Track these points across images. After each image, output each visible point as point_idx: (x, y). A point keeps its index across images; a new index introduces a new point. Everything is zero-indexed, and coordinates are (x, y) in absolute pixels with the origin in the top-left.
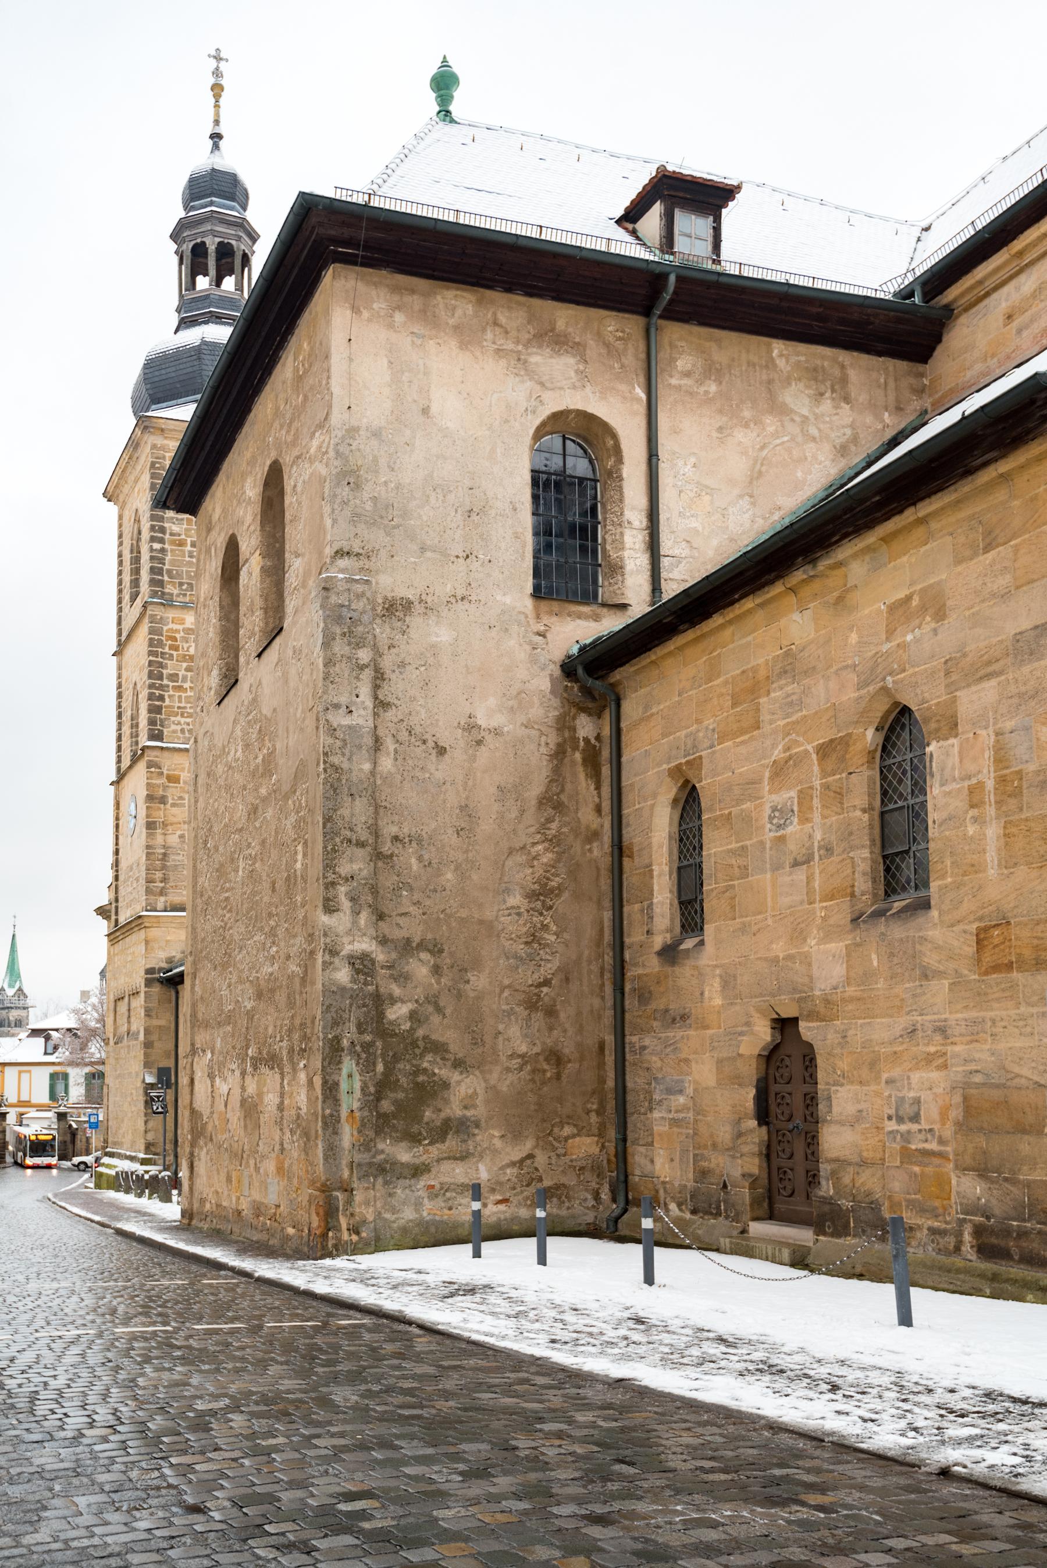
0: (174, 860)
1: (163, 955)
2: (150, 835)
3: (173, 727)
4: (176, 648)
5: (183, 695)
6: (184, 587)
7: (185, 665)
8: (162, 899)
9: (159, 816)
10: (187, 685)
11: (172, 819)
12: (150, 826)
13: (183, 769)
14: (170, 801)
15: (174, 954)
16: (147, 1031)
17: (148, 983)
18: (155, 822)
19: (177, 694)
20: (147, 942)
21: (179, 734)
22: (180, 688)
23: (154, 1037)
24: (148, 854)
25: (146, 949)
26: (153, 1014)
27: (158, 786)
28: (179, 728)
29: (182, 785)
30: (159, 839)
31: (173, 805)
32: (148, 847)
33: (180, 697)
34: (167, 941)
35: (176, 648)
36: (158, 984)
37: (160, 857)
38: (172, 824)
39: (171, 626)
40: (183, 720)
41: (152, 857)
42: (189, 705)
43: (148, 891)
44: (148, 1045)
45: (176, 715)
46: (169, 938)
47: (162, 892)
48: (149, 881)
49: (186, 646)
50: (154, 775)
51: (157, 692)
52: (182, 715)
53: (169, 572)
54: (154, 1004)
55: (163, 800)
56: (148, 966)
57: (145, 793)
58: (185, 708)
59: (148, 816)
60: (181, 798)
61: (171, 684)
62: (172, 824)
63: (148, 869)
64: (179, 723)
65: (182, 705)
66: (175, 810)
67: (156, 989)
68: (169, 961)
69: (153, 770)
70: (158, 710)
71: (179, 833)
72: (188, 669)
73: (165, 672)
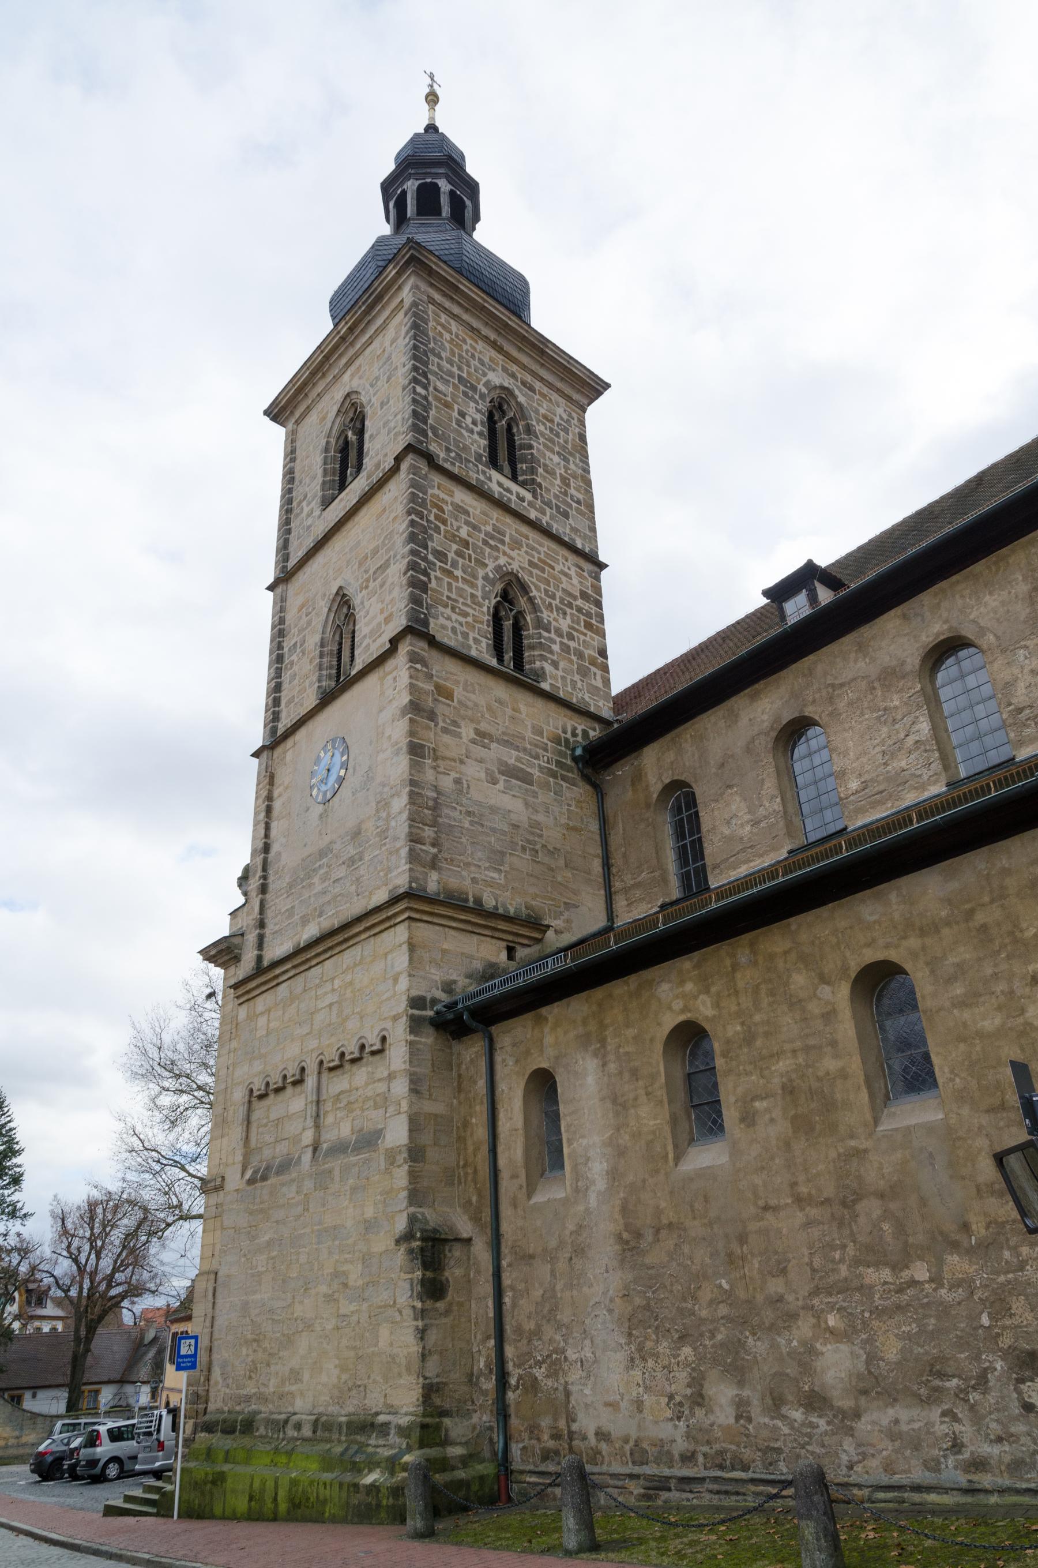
0: (449, 817)
1: (437, 975)
2: (415, 766)
3: (442, 621)
4: (444, 522)
5: (454, 584)
6: (453, 455)
7: (455, 547)
8: (434, 876)
9: (430, 737)
10: (458, 573)
11: (442, 751)
12: (416, 750)
13: (457, 682)
14: (441, 724)
15: (454, 977)
16: (415, 1126)
17: (415, 1025)
18: (422, 746)
19: (446, 579)
20: (412, 947)
21: (450, 633)
22: (449, 573)
23: (426, 1138)
24: (411, 794)
25: (411, 959)
26: (424, 1088)
27: (427, 693)
28: (449, 624)
29: (455, 703)
30: (430, 775)
31: (445, 730)
32: (413, 783)
33: (449, 584)
34: (444, 952)
35: (444, 522)
36: (430, 1030)
37: (431, 803)
38: (444, 758)
39: (436, 491)
40: (454, 617)
41: (419, 801)
42: (461, 600)
43: (413, 857)
44: (415, 1153)
45: (446, 606)
46: (445, 946)
47: (434, 864)
48: (414, 839)
49: (455, 524)
50: (420, 675)
51: (423, 564)
52: (453, 609)
53: (434, 430)
54: (424, 1070)
55: (432, 716)
56: (414, 993)
57: (405, 699)
58: (456, 601)
59: (412, 733)
60: (455, 723)
61: (438, 564)
62: (444, 758)
63: (411, 819)
64: (449, 618)
65: (453, 596)
66: (446, 739)
67: (428, 1038)
68: (448, 987)
69: (418, 666)
70: (424, 587)
71: (453, 775)
72: (459, 554)
73: (430, 544)
